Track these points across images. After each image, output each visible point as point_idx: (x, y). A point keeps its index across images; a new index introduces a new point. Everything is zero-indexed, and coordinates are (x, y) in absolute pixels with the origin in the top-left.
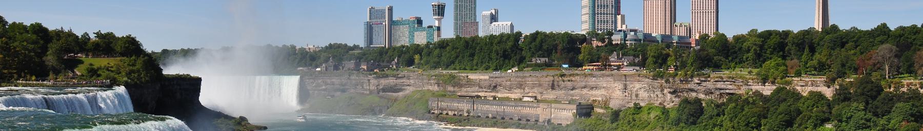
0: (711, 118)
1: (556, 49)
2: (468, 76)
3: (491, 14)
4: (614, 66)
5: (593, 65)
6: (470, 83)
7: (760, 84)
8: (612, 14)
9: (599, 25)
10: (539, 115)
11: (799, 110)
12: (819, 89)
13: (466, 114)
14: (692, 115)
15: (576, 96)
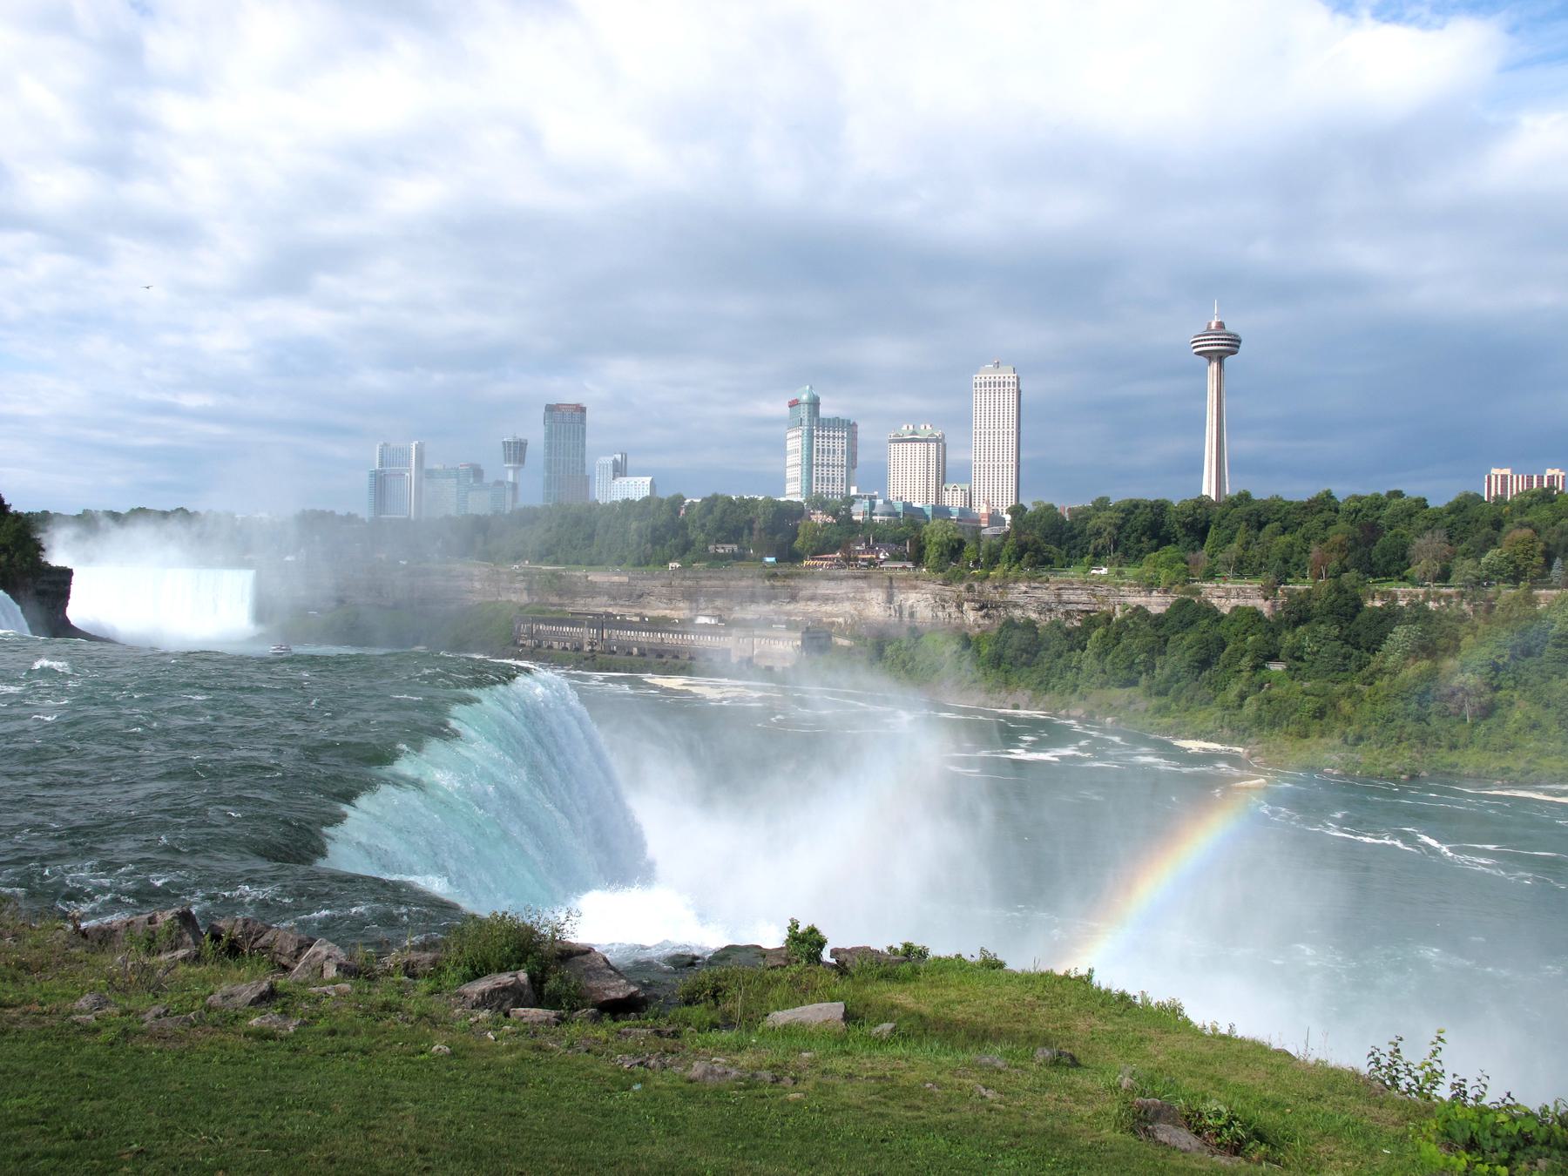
0: (1060, 656)
1: (751, 530)
2: (587, 577)
3: (615, 461)
4: (864, 560)
5: (821, 559)
6: (593, 590)
7: (1143, 594)
8: (842, 466)
9: (820, 486)
10: (730, 650)
11: (1222, 639)
12: (1250, 603)
13: (587, 648)
14: (1025, 651)
15: (796, 615)
